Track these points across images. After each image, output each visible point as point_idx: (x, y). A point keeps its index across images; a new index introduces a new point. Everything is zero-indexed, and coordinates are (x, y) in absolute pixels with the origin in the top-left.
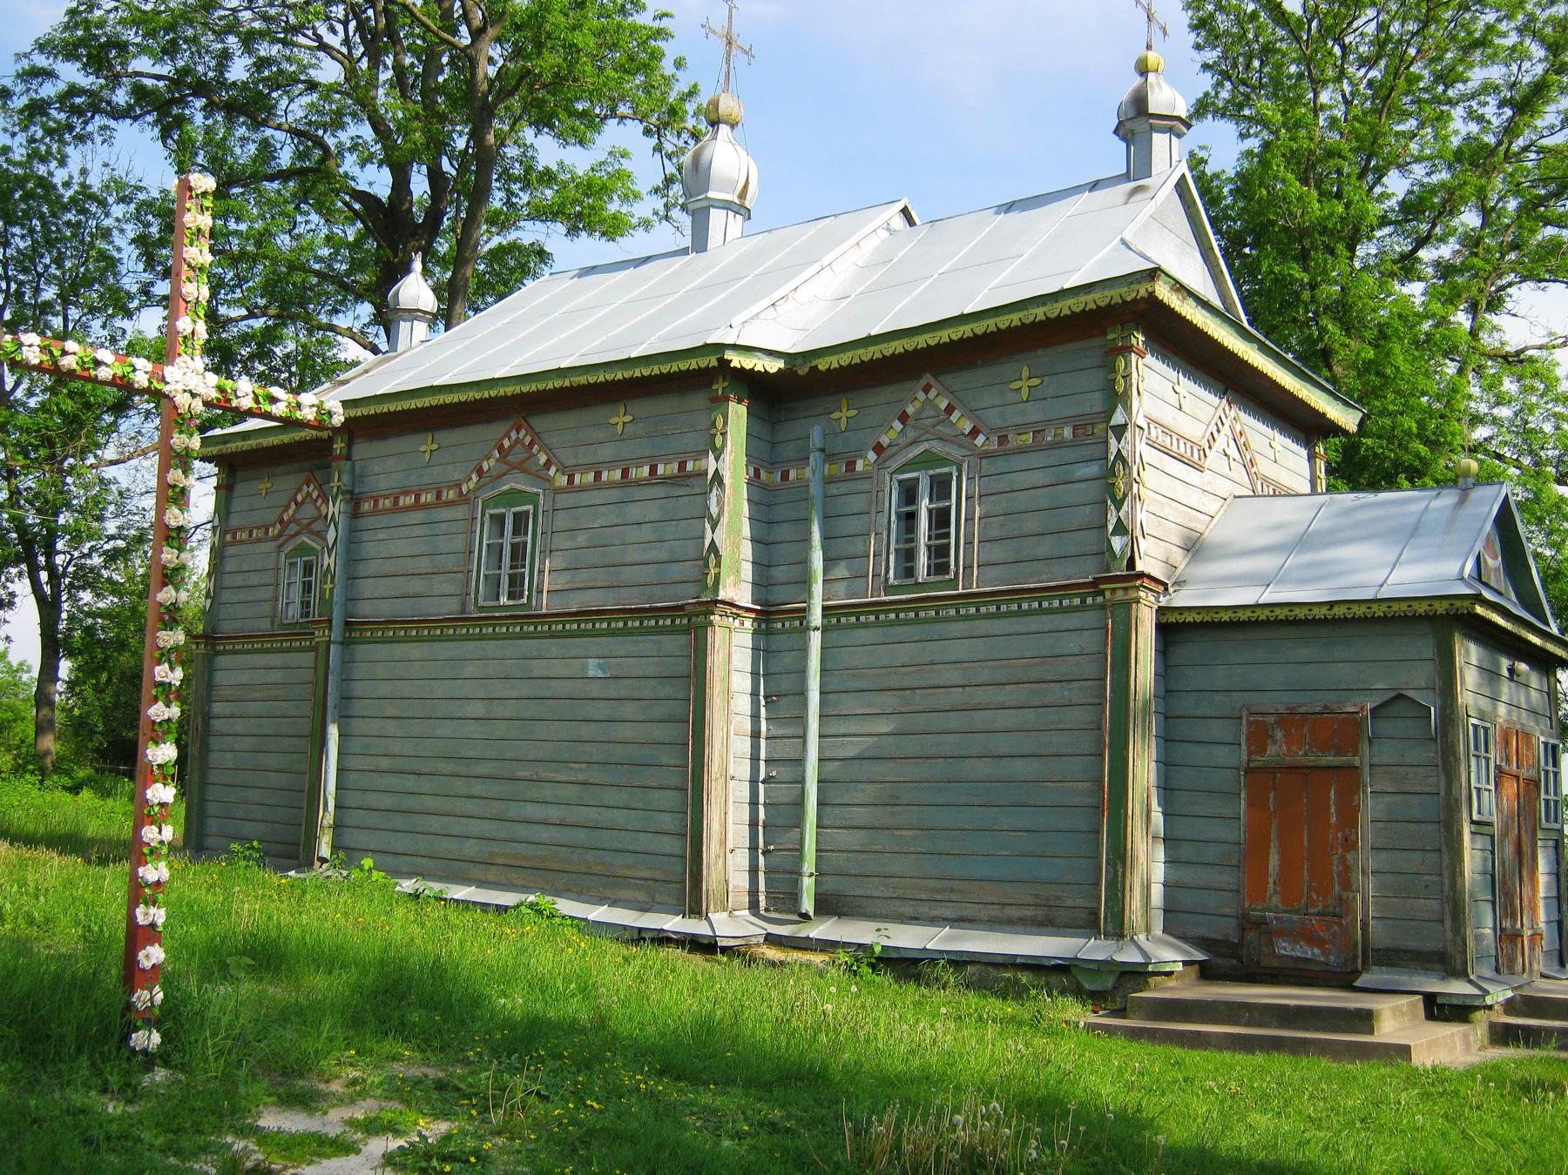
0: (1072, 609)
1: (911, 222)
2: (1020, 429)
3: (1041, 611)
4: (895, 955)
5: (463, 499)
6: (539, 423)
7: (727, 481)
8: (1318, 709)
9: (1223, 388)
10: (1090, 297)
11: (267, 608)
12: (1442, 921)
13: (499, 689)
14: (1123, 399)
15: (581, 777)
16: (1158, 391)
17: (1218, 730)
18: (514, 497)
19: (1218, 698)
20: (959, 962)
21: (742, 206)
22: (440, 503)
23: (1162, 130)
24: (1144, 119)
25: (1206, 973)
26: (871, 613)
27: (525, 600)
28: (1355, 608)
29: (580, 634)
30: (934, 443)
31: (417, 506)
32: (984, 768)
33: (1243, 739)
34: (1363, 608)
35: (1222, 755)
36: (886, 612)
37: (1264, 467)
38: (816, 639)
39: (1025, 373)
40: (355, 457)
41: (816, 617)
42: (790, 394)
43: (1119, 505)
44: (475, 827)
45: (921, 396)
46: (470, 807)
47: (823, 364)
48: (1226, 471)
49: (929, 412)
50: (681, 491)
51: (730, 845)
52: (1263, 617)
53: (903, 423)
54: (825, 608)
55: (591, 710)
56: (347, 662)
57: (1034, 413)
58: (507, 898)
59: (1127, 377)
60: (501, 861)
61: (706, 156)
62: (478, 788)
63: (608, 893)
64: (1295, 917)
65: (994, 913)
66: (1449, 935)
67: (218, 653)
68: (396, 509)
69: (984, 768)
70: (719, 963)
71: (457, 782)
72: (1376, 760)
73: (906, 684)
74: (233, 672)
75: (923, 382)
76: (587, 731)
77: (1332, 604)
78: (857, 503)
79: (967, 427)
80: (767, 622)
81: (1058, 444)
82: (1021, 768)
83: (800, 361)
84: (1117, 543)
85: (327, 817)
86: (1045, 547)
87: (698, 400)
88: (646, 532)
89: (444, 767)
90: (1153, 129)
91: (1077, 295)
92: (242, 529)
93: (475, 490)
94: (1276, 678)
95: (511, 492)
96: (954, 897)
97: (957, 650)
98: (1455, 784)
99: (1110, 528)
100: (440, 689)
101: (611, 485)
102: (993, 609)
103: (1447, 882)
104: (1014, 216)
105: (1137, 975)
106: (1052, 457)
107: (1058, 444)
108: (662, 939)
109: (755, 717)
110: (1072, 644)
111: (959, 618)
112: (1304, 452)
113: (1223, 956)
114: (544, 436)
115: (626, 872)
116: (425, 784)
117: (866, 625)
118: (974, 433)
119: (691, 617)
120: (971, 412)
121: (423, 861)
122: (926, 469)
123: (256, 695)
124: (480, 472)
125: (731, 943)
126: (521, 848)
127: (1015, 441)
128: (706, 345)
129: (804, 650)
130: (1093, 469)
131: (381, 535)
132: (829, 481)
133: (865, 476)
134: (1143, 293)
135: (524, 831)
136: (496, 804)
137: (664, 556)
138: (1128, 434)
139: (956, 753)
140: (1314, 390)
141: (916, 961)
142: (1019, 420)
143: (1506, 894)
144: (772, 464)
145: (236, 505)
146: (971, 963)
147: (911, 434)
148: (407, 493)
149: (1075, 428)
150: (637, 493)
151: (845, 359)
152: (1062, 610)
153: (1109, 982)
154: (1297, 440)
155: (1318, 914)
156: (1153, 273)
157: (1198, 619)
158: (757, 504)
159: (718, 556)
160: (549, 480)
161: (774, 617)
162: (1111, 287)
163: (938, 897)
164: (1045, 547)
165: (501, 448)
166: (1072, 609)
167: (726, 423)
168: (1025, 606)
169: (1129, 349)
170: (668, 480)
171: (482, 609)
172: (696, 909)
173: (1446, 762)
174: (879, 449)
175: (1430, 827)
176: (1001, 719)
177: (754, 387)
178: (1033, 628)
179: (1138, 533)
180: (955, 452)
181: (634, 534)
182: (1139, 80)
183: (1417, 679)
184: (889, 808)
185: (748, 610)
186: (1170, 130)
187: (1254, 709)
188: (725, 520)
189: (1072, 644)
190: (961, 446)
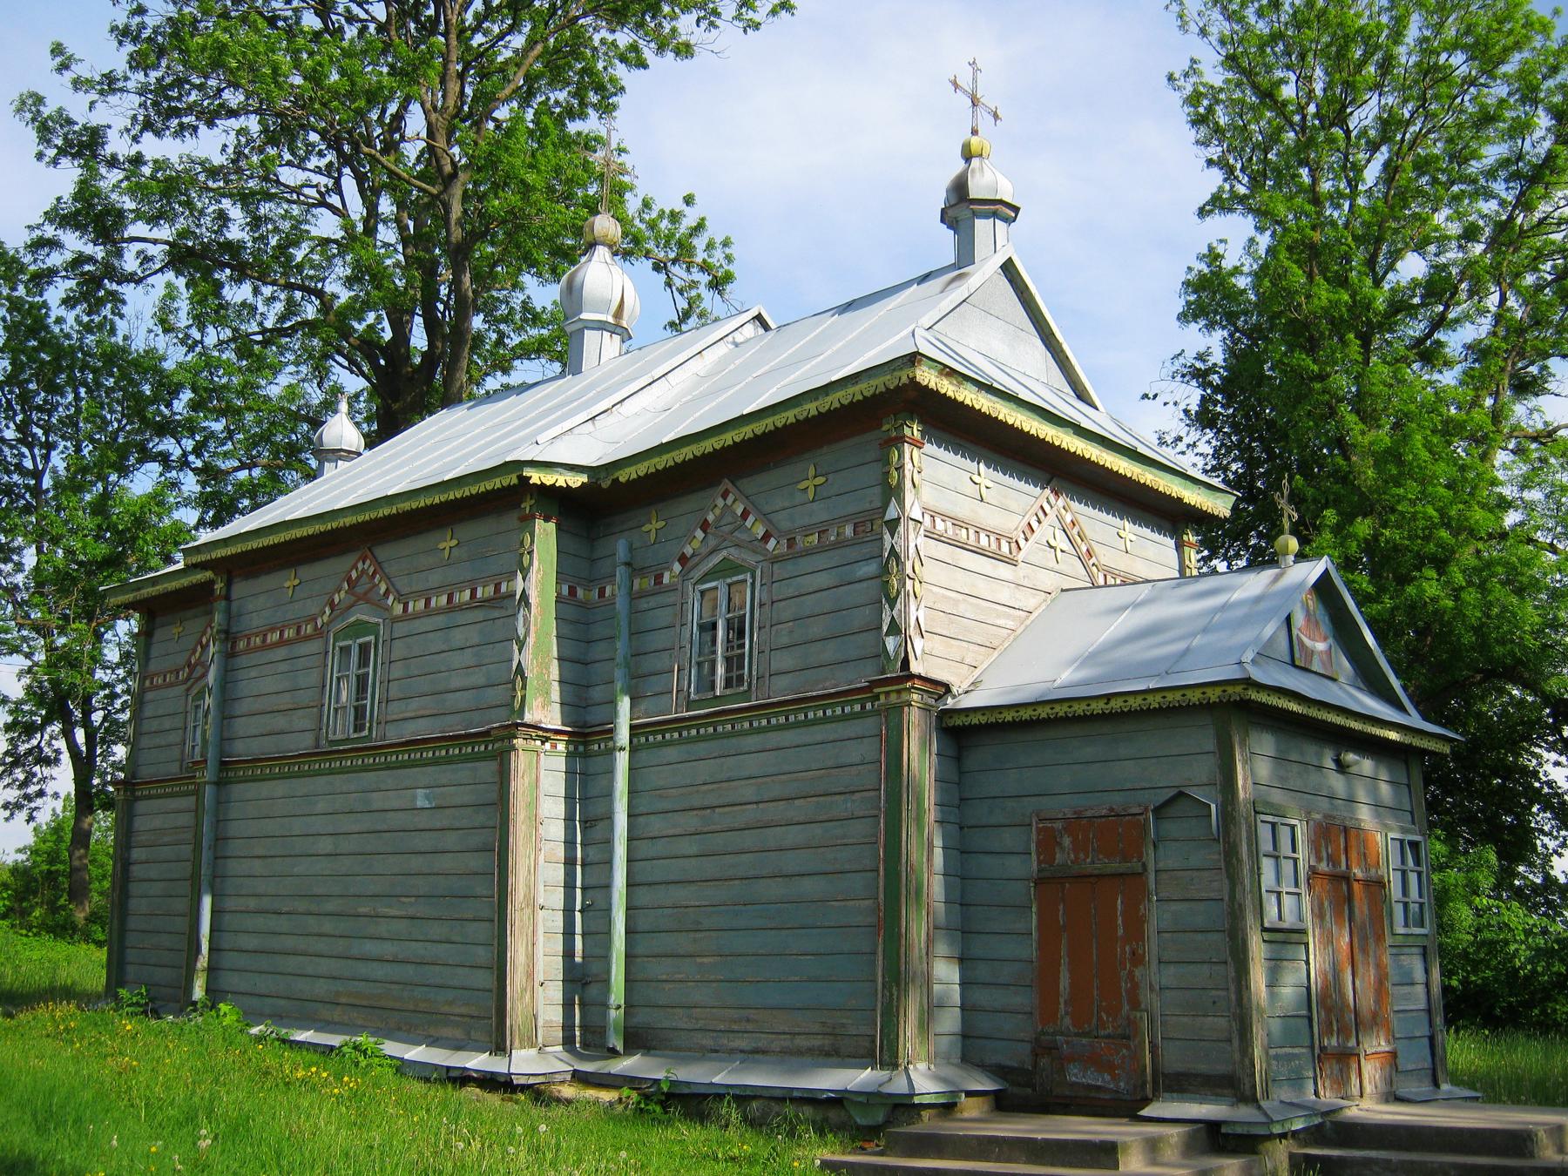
0: (854, 716)
1: (766, 327)
2: (807, 531)
3: (825, 720)
4: (686, 1091)
5: (319, 633)
6: (383, 552)
7: (533, 600)
8: (1104, 812)
9: (1048, 476)
10: (856, 388)
11: (176, 752)
12: (1229, 1041)
13: (347, 823)
14: (896, 492)
15: (411, 911)
16: (935, 478)
17: (1010, 839)
18: (360, 628)
19: (1010, 804)
20: (743, 1097)
21: (617, 325)
22: (301, 639)
23: (986, 216)
24: (964, 205)
25: (1002, 1104)
26: (675, 730)
27: (366, 733)
28: (1131, 701)
29: (411, 764)
30: (732, 550)
31: (283, 642)
32: (775, 889)
33: (1033, 847)
34: (1139, 700)
35: (1015, 866)
36: (689, 728)
37: (1105, 556)
38: (622, 760)
39: (812, 472)
40: (234, 595)
41: (623, 736)
42: (598, 507)
43: (892, 603)
44: (325, 966)
45: (720, 502)
46: (320, 945)
47: (623, 476)
48: (1052, 564)
49: (728, 519)
50: (496, 614)
51: (539, 977)
52: (1044, 715)
53: (705, 531)
54: (632, 727)
55: (420, 842)
56: (220, 802)
57: (820, 513)
58: (335, 1040)
59: (900, 468)
60: (343, 1000)
61: (578, 279)
62: (328, 926)
63: (432, 1031)
64: (1084, 1041)
65: (787, 1043)
66: (1237, 1056)
67: (138, 799)
68: (265, 647)
69: (775, 889)
70: (517, 1102)
71: (311, 920)
72: (1161, 865)
73: (706, 803)
74: (154, 816)
75: (721, 488)
76: (416, 863)
77: (1108, 697)
78: (664, 617)
79: (760, 531)
80: (586, 744)
81: (840, 544)
82: (809, 887)
83: (602, 475)
84: (891, 643)
85: (203, 962)
86: (829, 652)
87: (511, 520)
88: (467, 657)
89: (302, 905)
90: (976, 215)
91: (845, 386)
92: (158, 674)
93: (328, 624)
94: (1067, 780)
95: (359, 623)
96: (750, 1027)
97: (751, 764)
98: (1238, 889)
99: (885, 628)
100: (298, 826)
101: (440, 611)
102: (782, 720)
103: (1233, 997)
104: (847, 315)
105: (905, 1106)
106: (835, 557)
107: (840, 544)
108: (462, 1079)
109: (569, 843)
110: (854, 752)
111: (754, 731)
112: (1171, 543)
113: (1019, 1085)
114: (385, 565)
115: (446, 1009)
116: (283, 924)
117: (671, 743)
118: (766, 537)
119: (494, 742)
120: (765, 516)
121: (282, 1002)
122: (725, 577)
123: (166, 839)
124: (332, 606)
125: (532, 1081)
126: (361, 986)
127: (802, 543)
128: (506, 463)
129: (610, 771)
130: (871, 568)
131: (253, 673)
132: (634, 597)
133: (672, 589)
134: (904, 380)
135: (363, 969)
136: (342, 942)
137: (482, 681)
138: (901, 529)
139: (752, 873)
140: (1162, 474)
141: (706, 1096)
142: (806, 521)
143: (1329, 1010)
144: (589, 582)
145: (154, 652)
146: (755, 1097)
147: (712, 542)
148: (273, 630)
149: (856, 526)
150: (461, 618)
151: (642, 469)
152: (845, 718)
153: (880, 1117)
154: (1160, 529)
155: (1108, 1037)
156: (914, 358)
157: (983, 719)
158: (572, 622)
159: (524, 679)
160: (388, 609)
161: (585, 737)
162: (876, 376)
163: (735, 1027)
164: (829, 652)
165: (349, 580)
166: (854, 716)
167: (532, 542)
168: (811, 715)
169: (901, 440)
170: (487, 603)
171: (333, 742)
172: (499, 1047)
173: (1228, 863)
174: (683, 560)
175: (1215, 937)
176: (793, 835)
177: (558, 502)
178: (819, 738)
179: (912, 631)
180: (750, 559)
181: (457, 660)
182: (961, 164)
183: (1197, 774)
184: (692, 935)
185: (557, 732)
186: (995, 215)
187: (1043, 816)
188: (531, 640)
189: (854, 752)
190: (755, 552)
